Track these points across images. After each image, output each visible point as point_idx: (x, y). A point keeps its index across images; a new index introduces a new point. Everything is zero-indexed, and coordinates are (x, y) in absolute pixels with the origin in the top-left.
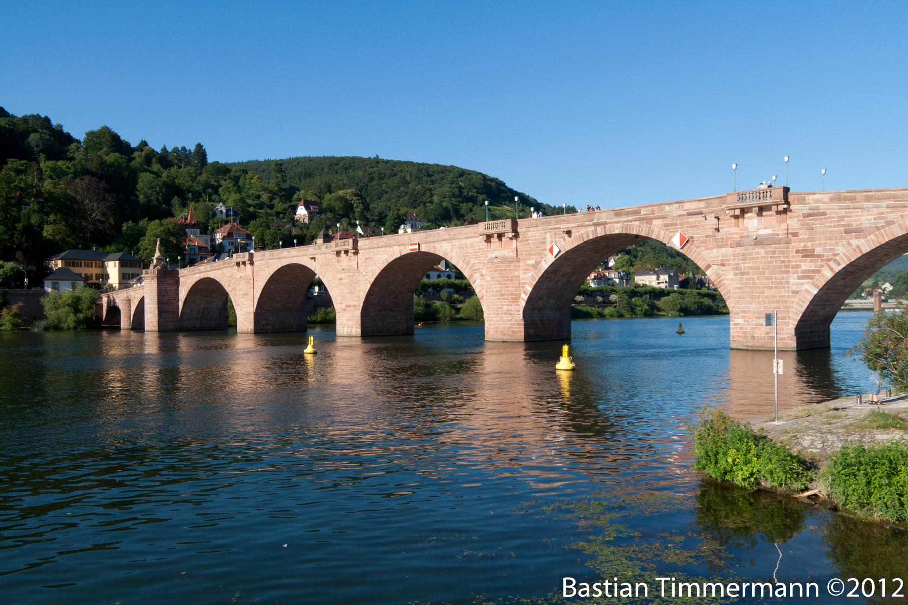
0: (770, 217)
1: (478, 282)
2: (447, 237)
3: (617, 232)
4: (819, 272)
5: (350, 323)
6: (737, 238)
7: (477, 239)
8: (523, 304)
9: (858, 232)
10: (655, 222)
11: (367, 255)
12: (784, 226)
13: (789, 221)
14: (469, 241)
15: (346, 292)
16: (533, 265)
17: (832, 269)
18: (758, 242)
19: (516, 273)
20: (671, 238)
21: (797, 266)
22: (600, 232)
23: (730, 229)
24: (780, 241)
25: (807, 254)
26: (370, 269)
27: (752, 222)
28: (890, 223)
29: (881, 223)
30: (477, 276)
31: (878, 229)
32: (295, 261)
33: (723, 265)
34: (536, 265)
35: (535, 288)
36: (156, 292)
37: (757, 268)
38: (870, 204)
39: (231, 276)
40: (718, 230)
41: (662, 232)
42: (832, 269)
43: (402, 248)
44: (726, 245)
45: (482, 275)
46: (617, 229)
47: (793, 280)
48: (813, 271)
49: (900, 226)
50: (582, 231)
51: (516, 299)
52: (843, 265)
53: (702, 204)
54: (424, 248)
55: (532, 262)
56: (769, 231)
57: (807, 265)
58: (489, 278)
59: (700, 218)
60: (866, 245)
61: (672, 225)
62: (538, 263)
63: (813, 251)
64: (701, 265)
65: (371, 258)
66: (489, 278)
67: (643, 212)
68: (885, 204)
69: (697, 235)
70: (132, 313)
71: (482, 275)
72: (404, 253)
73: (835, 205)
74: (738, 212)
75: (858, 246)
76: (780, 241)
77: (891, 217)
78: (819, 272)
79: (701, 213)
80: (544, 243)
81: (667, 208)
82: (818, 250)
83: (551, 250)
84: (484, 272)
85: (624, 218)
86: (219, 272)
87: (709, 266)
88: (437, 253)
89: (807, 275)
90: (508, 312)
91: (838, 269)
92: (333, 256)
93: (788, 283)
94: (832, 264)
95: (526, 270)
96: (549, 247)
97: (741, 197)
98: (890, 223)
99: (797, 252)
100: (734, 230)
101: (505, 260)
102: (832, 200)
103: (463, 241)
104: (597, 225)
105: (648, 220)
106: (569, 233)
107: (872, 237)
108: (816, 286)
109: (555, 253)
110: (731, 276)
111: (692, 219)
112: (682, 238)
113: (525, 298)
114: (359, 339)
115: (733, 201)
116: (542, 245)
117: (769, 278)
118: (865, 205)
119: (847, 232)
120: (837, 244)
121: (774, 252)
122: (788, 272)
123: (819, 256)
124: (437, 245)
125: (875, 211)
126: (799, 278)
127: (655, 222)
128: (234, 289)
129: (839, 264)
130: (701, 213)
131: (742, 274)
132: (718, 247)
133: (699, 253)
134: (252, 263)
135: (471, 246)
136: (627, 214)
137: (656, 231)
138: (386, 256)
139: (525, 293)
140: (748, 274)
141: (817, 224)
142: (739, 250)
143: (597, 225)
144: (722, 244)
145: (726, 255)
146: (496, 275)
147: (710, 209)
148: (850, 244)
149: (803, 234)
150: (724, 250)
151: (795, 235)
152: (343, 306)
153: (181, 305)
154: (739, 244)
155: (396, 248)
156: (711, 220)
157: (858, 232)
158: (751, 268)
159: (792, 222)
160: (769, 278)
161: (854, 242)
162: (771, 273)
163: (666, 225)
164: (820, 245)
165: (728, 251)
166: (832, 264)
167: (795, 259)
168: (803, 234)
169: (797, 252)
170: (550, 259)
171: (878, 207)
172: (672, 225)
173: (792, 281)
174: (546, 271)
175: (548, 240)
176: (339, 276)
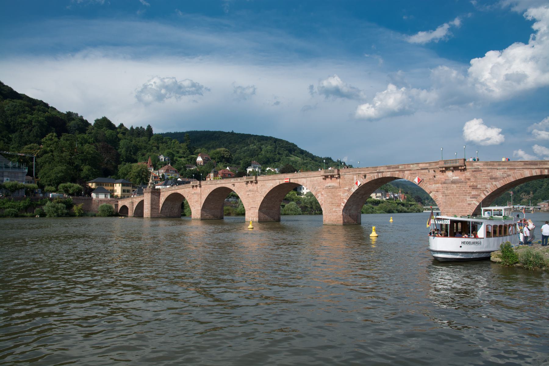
0: (458, 172)
1: (320, 197)
2: (304, 176)
3: (388, 176)
4: (479, 195)
5: (253, 216)
6: (443, 180)
7: (319, 178)
8: (342, 208)
9: (496, 179)
10: (406, 172)
11: (262, 184)
12: (464, 175)
13: (466, 173)
15: (251, 201)
16: (347, 190)
17: (485, 194)
18: (454, 182)
19: (339, 194)
20: (414, 179)
21: (470, 193)
22: (380, 176)
24: (462, 182)
25: (474, 188)
26: (263, 190)
27: (449, 174)
28: (509, 176)
29: (505, 175)
30: (319, 194)
31: (504, 178)
32: (224, 185)
33: (437, 192)
34: (350, 189)
35: (348, 201)
36: (150, 199)
37: (453, 193)
38: (500, 167)
39: (189, 192)
40: (435, 176)
41: (409, 177)
42: (485, 194)
44: (438, 183)
45: (322, 194)
46: (388, 175)
47: (468, 199)
48: (477, 195)
49: (513, 177)
50: (372, 175)
51: (339, 206)
52: (490, 193)
53: (428, 165)
54: (292, 181)
55: (347, 188)
56: (457, 178)
57: (474, 192)
58: (326, 196)
59: (427, 171)
60: (499, 184)
61: (414, 173)
62: (350, 189)
63: (477, 186)
64: (428, 191)
66: (326, 196)
67: (400, 167)
68: (506, 167)
69: (426, 178)
70: (134, 209)
71: (322, 194)
72: (281, 183)
73: (486, 167)
74: (444, 169)
75: (496, 185)
76: (462, 182)
77: (509, 173)
78: (479, 195)
79: (427, 169)
80: (353, 180)
81: (411, 166)
82: (479, 186)
83: (357, 183)
84: (323, 193)
85: (391, 170)
87: (431, 192)
89: (474, 197)
90: (335, 212)
91: (487, 194)
92: (244, 184)
93: (466, 200)
94: (485, 192)
95: (344, 192)
96: (355, 182)
97: (446, 162)
98: (509, 176)
99: (470, 187)
100: (443, 177)
101: (334, 187)
102: (484, 165)
103: (312, 178)
104: (378, 172)
106: (365, 176)
107: (502, 181)
108: (478, 202)
109: (359, 185)
110: (441, 196)
111: (423, 171)
112: (419, 180)
113: (344, 205)
115: (442, 164)
116: (353, 182)
117: (459, 198)
118: (498, 167)
119: (491, 179)
120: (487, 184)
121: (460, 187)
122: (466, 195)
123: (479, 189)
124: (299, 180)
125: (503, 170)
126: (471, 198)
128: (190, 198)
129: (488, 192)
130: (427, 169)
131: (446, 196)
132: (435, 184)
133: (426, 186)
134: (200, 187)
135: (317, 180)
136: (393, 168)
137: (406, 176)
138: (272, 184)
139: (343, 203)
140: (449, 196)
141: (478, 175)
142: (445, 185)
143: (378, 172)
144: (436, 182)
145: (439, 187)
146: (330, 194)
147: (431, 167)
148: (492, 184)
149: (472, 179)
150: (437, 185)
151: (469, 179)
152: (249, 207)
153: (161, 205)
154: (445, 183)
155: (278, 181)
156: (432, 171)
157: (496, 179)
158: (450, 193)
159: (467, 174)
160: (459, 198)
161: (494, 183)
162: (459, 195)
163: (411, 174)
164: (480, 184)
165: (440, 185)
166: (485, 192)
167: (469, 190)
168: (472, 179)
169: (470, 187)
170: (356, 188)
171: (504, 169)
172: (414, 173)
173: (468, 199)
174: (354, 193)
175: (355, 179)
176: (248, 193)
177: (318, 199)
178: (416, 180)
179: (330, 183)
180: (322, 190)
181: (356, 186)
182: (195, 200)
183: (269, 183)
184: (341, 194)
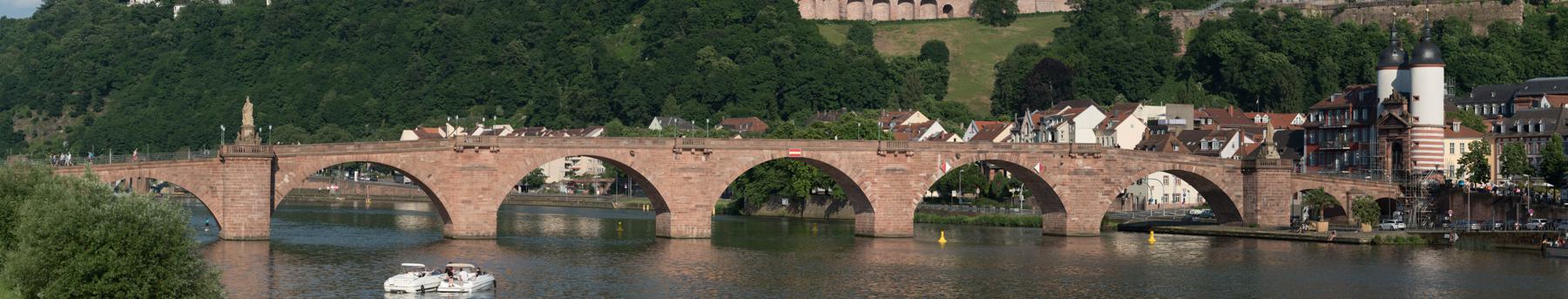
0: (1090, 160)
18: (1089, 173)
23: (1068, 164)
25: (1107, 182)
27: (1080, 162)
57: (1107, 188)
62: (928, 177)
72: (777, 157)
95: (918, 181)
105: (1017, 153)
114: (708, 243)
141: (1112, 165)
156: (1058, 157)
159: (1100, 164)
167: (1101, 184)
170: (941, 174)
178: (1037, 168)
179: (889, 162)
182: (480, 186)
183: (740, 155)
184: (912, 183)
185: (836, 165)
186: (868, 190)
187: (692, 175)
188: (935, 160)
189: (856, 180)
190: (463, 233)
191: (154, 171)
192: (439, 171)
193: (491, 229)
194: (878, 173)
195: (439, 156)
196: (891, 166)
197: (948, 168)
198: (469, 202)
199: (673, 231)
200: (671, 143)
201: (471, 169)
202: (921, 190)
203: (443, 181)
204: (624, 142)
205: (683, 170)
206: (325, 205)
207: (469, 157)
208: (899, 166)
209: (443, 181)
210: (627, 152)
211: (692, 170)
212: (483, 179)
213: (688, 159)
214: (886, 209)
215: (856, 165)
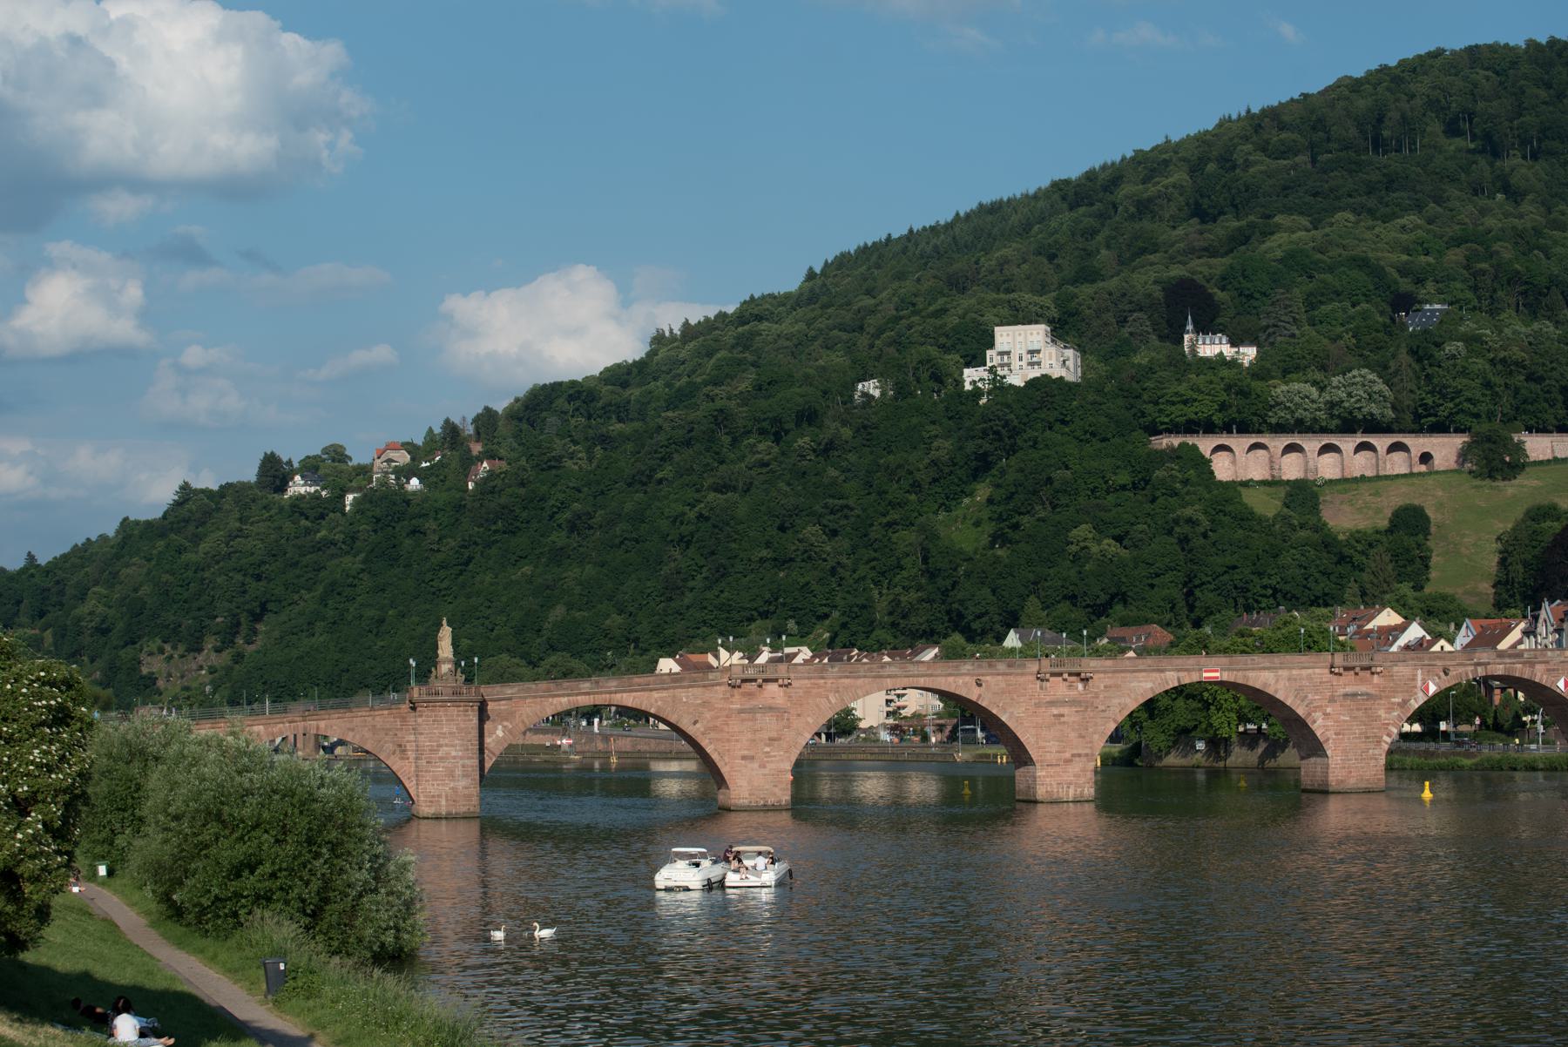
1: (1320, 722)
8: (1386, 747)
10: (1538, 667)
11: (1108, 682)
14: (1304, 672)
26: (1116, 701)
30: (1318, 715)
34: (1405, 702)
39: (705, 704)
43: (1181, 674)
50: (1461, 670)
62: (1405, 702)
65: (1117, 686)
72: (1186, 681)
84: (1329, 710)
86: (655, 695)
88: (1250, 683)
95: (1390, 710)
105: (1532, 664)
109: (1431, 692)
114: (1092, 805)
124: (1251, 674)
127: (1538, 667)
135: (1309, 678)
138: (1149, 685)
139: (1389, 735)
152: (1067, 755)
175: (1419, 677)
177: (1314, 727)
178: (1561, 684)
179: (1348, 684)
180: (1325, 702)
181: (1420, 694)
182: (766, 735)
183: (1132, 680)
184: (1382, 713)
185: (1270, 691)
186: (1319, 726)
187: (1065, 710)
188: (1414, 679)
189: (1301, 711)
190: (746, 802)
191: (322, 724)
192: (708, 715)
193: (785, 797)
194: (1332, 700)
195: (708, 694)
196: (1349, 690)
197: (1433, 689)
198: (752, 758)
199: (1041, 792)
200: (1033, 667)
201: (753, 711)
202: (1395, 722)
203: (715, 728)
204: (967, 667)
205: (1052, 703)
206: (556, 768)
207: (750, 695)
208: (1362, 689)
209: (715, 728)
210: (971, 680)
211: (1063, 703)
212: (769, 724)
213: (1058, 688)
214: (1345, 751)
215: (1299, 690)
